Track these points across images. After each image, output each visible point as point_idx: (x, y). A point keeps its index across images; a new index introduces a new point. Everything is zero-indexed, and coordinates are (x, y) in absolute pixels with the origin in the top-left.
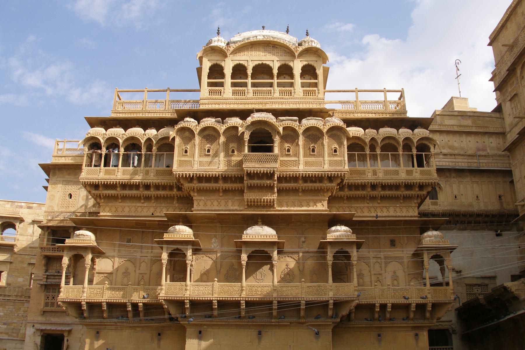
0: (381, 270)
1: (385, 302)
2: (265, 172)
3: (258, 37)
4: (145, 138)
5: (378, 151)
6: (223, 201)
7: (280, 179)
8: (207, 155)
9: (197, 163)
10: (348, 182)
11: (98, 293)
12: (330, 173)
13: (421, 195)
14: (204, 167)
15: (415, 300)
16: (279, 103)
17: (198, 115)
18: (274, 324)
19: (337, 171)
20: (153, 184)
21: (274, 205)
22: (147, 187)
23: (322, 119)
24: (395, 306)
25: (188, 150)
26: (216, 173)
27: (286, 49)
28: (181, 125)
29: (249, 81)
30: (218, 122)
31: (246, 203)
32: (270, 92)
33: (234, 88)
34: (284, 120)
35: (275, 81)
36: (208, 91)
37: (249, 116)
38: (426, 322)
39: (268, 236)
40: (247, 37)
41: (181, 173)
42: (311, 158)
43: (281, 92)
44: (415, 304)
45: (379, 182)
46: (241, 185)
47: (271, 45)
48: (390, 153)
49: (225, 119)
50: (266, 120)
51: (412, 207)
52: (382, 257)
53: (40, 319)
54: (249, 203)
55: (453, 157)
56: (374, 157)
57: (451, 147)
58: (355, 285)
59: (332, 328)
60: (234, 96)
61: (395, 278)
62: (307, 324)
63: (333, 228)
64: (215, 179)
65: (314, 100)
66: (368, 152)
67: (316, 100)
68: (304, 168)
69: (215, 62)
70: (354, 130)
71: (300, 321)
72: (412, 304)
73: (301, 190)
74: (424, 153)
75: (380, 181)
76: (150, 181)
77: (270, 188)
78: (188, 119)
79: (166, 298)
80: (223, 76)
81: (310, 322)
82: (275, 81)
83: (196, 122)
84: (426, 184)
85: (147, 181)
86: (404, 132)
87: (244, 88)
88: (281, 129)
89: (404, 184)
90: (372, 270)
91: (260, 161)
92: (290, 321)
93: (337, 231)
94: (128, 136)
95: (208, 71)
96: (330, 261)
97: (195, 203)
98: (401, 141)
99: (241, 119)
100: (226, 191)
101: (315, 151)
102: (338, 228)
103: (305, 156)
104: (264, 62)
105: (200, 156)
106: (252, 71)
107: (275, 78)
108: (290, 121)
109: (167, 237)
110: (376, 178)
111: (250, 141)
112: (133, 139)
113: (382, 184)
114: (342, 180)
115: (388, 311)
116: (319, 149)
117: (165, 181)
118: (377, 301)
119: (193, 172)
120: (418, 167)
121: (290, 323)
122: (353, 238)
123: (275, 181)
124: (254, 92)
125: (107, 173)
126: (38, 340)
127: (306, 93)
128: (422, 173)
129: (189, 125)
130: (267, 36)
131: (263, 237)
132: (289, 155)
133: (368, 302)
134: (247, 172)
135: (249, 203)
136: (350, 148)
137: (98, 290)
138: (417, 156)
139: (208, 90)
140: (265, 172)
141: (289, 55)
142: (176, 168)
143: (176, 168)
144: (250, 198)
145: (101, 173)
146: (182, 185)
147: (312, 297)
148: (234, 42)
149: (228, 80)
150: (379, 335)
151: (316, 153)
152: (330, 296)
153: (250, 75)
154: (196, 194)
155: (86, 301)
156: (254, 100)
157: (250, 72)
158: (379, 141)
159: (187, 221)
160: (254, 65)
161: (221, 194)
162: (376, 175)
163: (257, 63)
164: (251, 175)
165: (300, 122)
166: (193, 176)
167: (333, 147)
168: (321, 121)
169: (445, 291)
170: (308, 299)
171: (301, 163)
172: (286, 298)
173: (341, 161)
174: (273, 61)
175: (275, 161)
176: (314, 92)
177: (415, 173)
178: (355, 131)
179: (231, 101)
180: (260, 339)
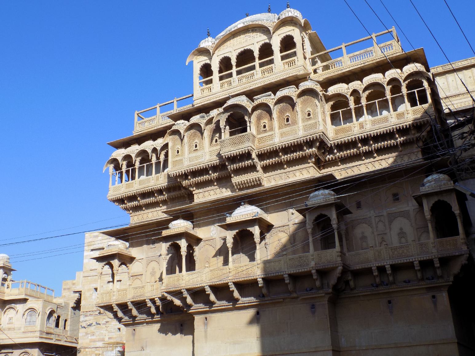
1: (382, 264)
5: (364, 102)
7: (261, 156)
9: (187, 160)
10: (334, 143)
11: (125, 294)
12: (304, 138)
13: (420, 138)
14: (193, 162)
17: (186, 116)
18: (268, 302)
19: (311, 135)
21: (261, 184)
22: (160, 192)
24: (395, 268)
29: (234, 70)
30: (203, 117)
33: (221, 82)
38: (441, 281)
41: (174, 172)
42: (286, 129)
43: (263, 72)
44: (418, 262)
46: (226, 172)
47: (249, 29)
50: (237, 103)
51: (414, 153)
52: (385, 214)
59: (327, 300)
61: (402, 234)
62: (301, 298)
66: (352, 105)
67: (296, 69)
68: (279, 139)
69: (204, 63)
70: (336, 87)
71: (292, 296)
72: (414, 262)
76: (159, 185)
77: (252, 168)
78: (178, 122)
79: (165, 290)
81: (302, 296)
82: (257, 62)
83: (186, 122)
84: (424, 122)
86: (392, 73)
89: (395, 130)
92: (282, 297)
93: (316, 196)
96: (309, 228)
97: (195, 197)
101: (290, 120)
103: (280, 128)
104: (246, 48)
106: (235, 60)
108: (265, 97)
109: (165, 233)
110: (362, 131)
112: (145, 152)
113: (371, 136)
117: (170, 183)
118: (373, 264)
121: (283, 299)
123: (254, 159)
124: (239, 79)
125: (128, 186)
129: (178, 127)
130: (246, 22)
133: (363, 267)
134: (225, 157)
137: (125, 292)
138: (408, 94)
139: (200, 90)
141: (267, 33)
144: (237, 181)
145: (123, 188)
147: (293, 271)
149: (216, 76)
150: (390, 302)
152: (312, 266)
153: (235, 64)
154: (194, 188)
157: (234, 62)
159: (188, 216)
160: (237, 54)
163: (239, 51)
165: (275, 95)
166: (185, 172)
167: (306, 111)
168: (294, 89)
170: (289, 272)
175: (248, 140)
176: (293, 62)
177: (407, 114)
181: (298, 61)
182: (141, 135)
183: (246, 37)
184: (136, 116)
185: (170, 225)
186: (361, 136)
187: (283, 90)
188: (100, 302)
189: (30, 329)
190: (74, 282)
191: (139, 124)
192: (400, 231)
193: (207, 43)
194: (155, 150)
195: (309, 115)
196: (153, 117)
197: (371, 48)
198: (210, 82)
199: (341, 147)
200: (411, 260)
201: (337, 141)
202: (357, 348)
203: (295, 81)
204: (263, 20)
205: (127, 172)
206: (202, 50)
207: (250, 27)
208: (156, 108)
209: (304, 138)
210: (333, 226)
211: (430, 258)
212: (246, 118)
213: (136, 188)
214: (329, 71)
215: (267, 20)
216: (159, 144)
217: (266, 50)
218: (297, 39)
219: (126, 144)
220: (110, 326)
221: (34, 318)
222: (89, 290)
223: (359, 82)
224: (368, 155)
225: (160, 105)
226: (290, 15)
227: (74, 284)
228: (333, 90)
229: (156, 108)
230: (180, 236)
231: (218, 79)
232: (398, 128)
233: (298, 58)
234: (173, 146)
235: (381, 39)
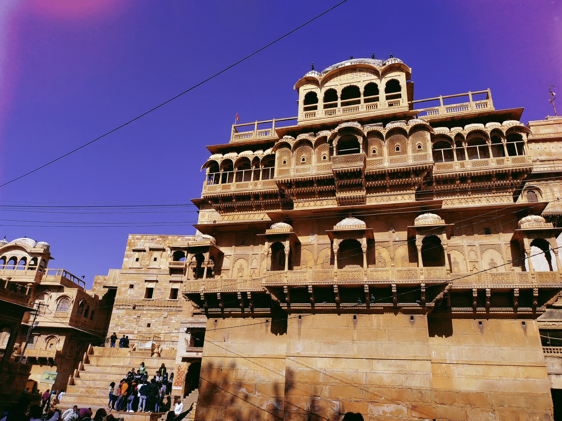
0: (477, 258)
2: (352, 170)
12: (414, 166)
15: (517, 285)
17: (294, 133)
20: (260, 194)
23: (405, 121)
26: (310, 177)
29: (339, 101)
30: (311, 135)
33: (326, 109)
36: (304, 115)
39: (357, 226)
41: (280, 180)
43: (368, 107)
44: (518, 289)
45: (468, 173)
47: (357, 69)
48: (477, 146)
52: (477, 245)
53: (191, 319)
55: (552, 162)
57: (550, 154)
58: (447, 269)
63: (420, 216)
65: (398, 109)
74: (515, 142)
75: (468, 172)
76: (258, 191)
77: (358, 187)
79: (267, 285)
80: (316, 101)
82: (362, 98)
83: (293, 138)
85: (256, 191)
87: (334, 108)
88: (366, 134)
90: (467, 257)
92: (383, 305)
93: (426, 218)
97: (295, 205)
98: (489, 133)
101: (400, 149)
103: (390, 154)
104: (352, 84)
107: (362, 96)
108: (375, 127)
109: (268, 232)
115: (487, 297)
116: (403, 147)
118: (474, 286)
119: (290, 178)
120: (509, 156)
122: (442, 223)
125: (224, 188)
126: (188, 337)
128: (514, 161)
131: (352, 227)
137: (214, 283)
138: (507, 145)
140: (352, 170)
142: (276, 176)
143: (276, 176)
149: (320, 104)
151: (400, 150)
152: (421, 280)
155: (204, 292)
157: (339, 94)
158: (465, 137)
160: (343, 88)
162: (464, 167)
163: (345, 86)
164: (341, 175)
165: (384, 126)
167: (417, 144)
168: (404, 123)
169: (554, 276)
170: (398, 283)
171: (386, 161)
172: (376, 282)
173: (426, 155)
174: (360, 82)
177: (506, 161)
178: (438, 130)
180: (355, 324)
182: (241, 144)
183: (353, 75)
184: (233, 129)
186: (462, 174)
187: (394, 123)
188: (187, 290)
189: (60, 314)
190: (106, 278)
191: (235, 136)
192: (491, 261)
193: (312, 74)
194: (256, 159)
195: (419, 147)
196: (250, 132)
197: (467, 103)
198: (315, 108)
200: (512, 287)
201: (439, 174)
202: (448, 362)
203: (406, 117)
204: (370, 63)
205: (224, 175)
206: (309, 79)
207: (358, 67)
208: (255, 124)
209: (414, 166)
210: (444, 246)
211: (531, 287)
212: (360, 140)
214: (426, 116)
216: (260, 155)
217: (372, 89)
219: (224, 151)
220: (141, 320)
221: (66, 306)
222: (125, 286)
223: (461, 128)
224: (464, 192)
225: (258, 122)
226: (396, 62)
227: (105, 280)
228: (438, 130)
229: (255, 124)
230: (284, 237)
232: (498, 172)
233: (403, 100)
234: (280, 158)
235: (476, 98)
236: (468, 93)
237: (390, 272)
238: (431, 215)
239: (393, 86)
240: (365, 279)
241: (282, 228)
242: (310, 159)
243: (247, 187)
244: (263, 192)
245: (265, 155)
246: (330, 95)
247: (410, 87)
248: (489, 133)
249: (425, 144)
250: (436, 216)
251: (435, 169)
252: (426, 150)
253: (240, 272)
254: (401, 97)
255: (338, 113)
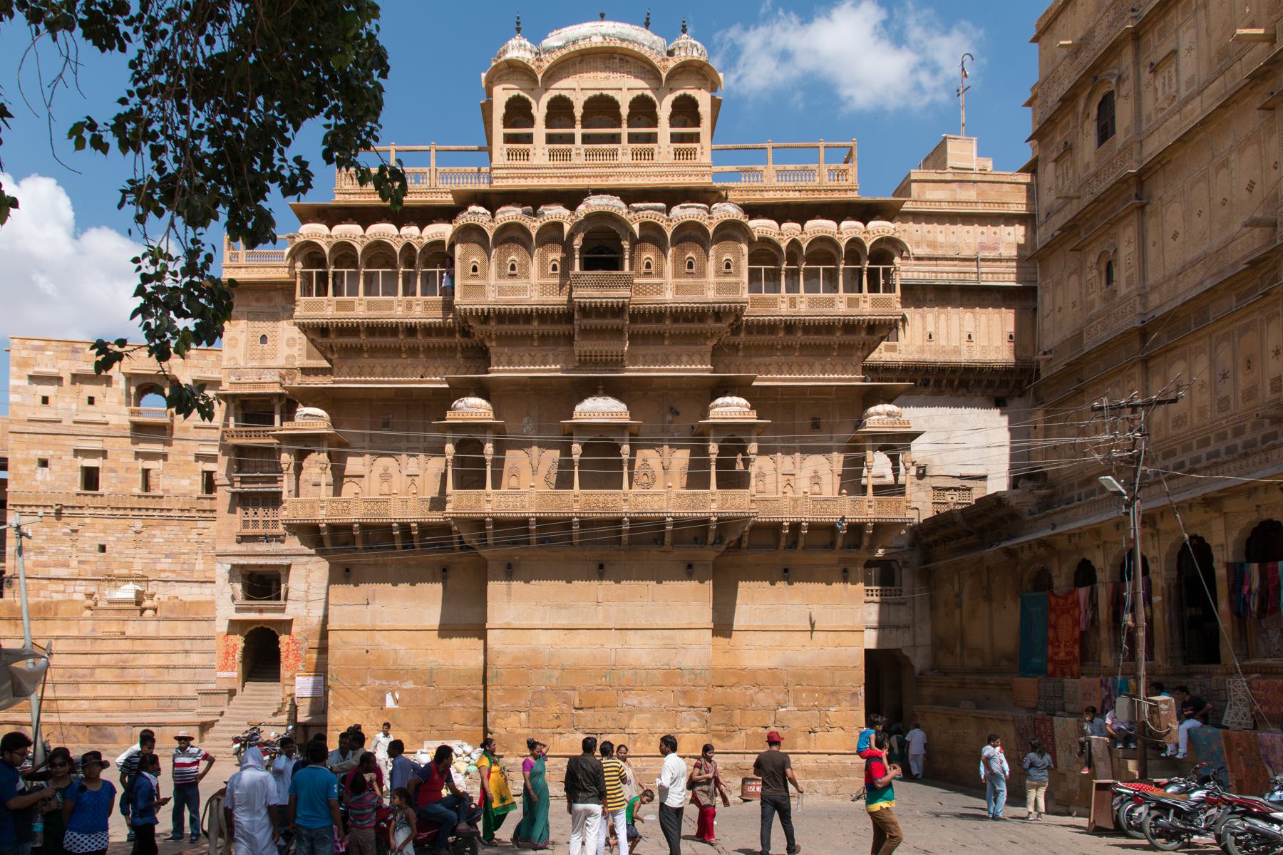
3: (594, 39)
4: (403, 242)
6: (539, 355)
8: (510, 275)
16: (631, 175)
17: (492, 200)
21: (622, 360)
25: (478, 267)
27: (645, 65)
28: (463, 219)
29: (578, 131)
31: (577, 358)
32: (614, 153)
33: (551, 146)
34: (641, 210)
35: (624, 131)
36: (506, 153)
37: (580, 202)
40: (572, 39)
41: (468, 307)
42: (685, 280)
46: (569, 327)
49: (539, 207)
54: (583, 358)
56: (792, 275)
60: (551, 163)
63: (719, 401)
64: (524, 317)
65: (693, 169)
67: (699, 169)
69: (515, 93)
73: (667, 335)
77: (618, 333)
78: (473, 208)
80: (530, 121)
82: (624, 131)
83: (489, 213)
91: (599, 285)
94: (371, 240)
95: (504, 111)
98: (843, 244)
99: (566, 207)
100: (544, 338)
102: (728, 399)
103: (676, 275)
104: (605, 92)
105: (500, 277)
109: (451, 417)
111: (581, 250)
114: (738, 317)
122: (752, 417)
127: (678, 153)
130: (609, 36)
132: (648, 274)
134: (580, 306)
135: (583, 358)
136: (752, 261)
146: (470, 326)
148: (549, 51)
149: (539, 130)
154: (494, 344)
156: (585, 170)
157: (578, 112)
158: (805, 246)
159: (482, 389)
160: (586, 98)
161: (535, 344)
163: (591, 94)
164: (588, 311)
165: (668, 211)
166: (489, 312)
168: (705, 212)
173: (737, 284)
174: (621, 89)
179: (550, 171)
181: (702, 153)
185: (458, 404)
193: (518, 49)
194: (408, 247)
195: (728, 266)
199: (769, 328)
203: (706, 196)
204: (644, 45)
213: (362, 314)
215: (651, 48)
217: (643, 110)
218: (705, 109)
223: (798, 226)
230: (483, 427)
231: (544, 138)
234: (464, 258)
236: (819, 144)
237: (665, 497)
238: (736, 400)
239: (686, 111)
240: (625, 508)
241: (473, 408)
242: (525, 267)
243: (391, 308)
244: (425, 324)
245: (426, 241)
246: (560, 110)
247: (716, 105)
248: (843, 244)
249: (738, 260)
250: (743, 401)
251: (748, 310)
252: (738, 274)
253: (386, 480)
254: (698, 141)
255: (578, 160)
